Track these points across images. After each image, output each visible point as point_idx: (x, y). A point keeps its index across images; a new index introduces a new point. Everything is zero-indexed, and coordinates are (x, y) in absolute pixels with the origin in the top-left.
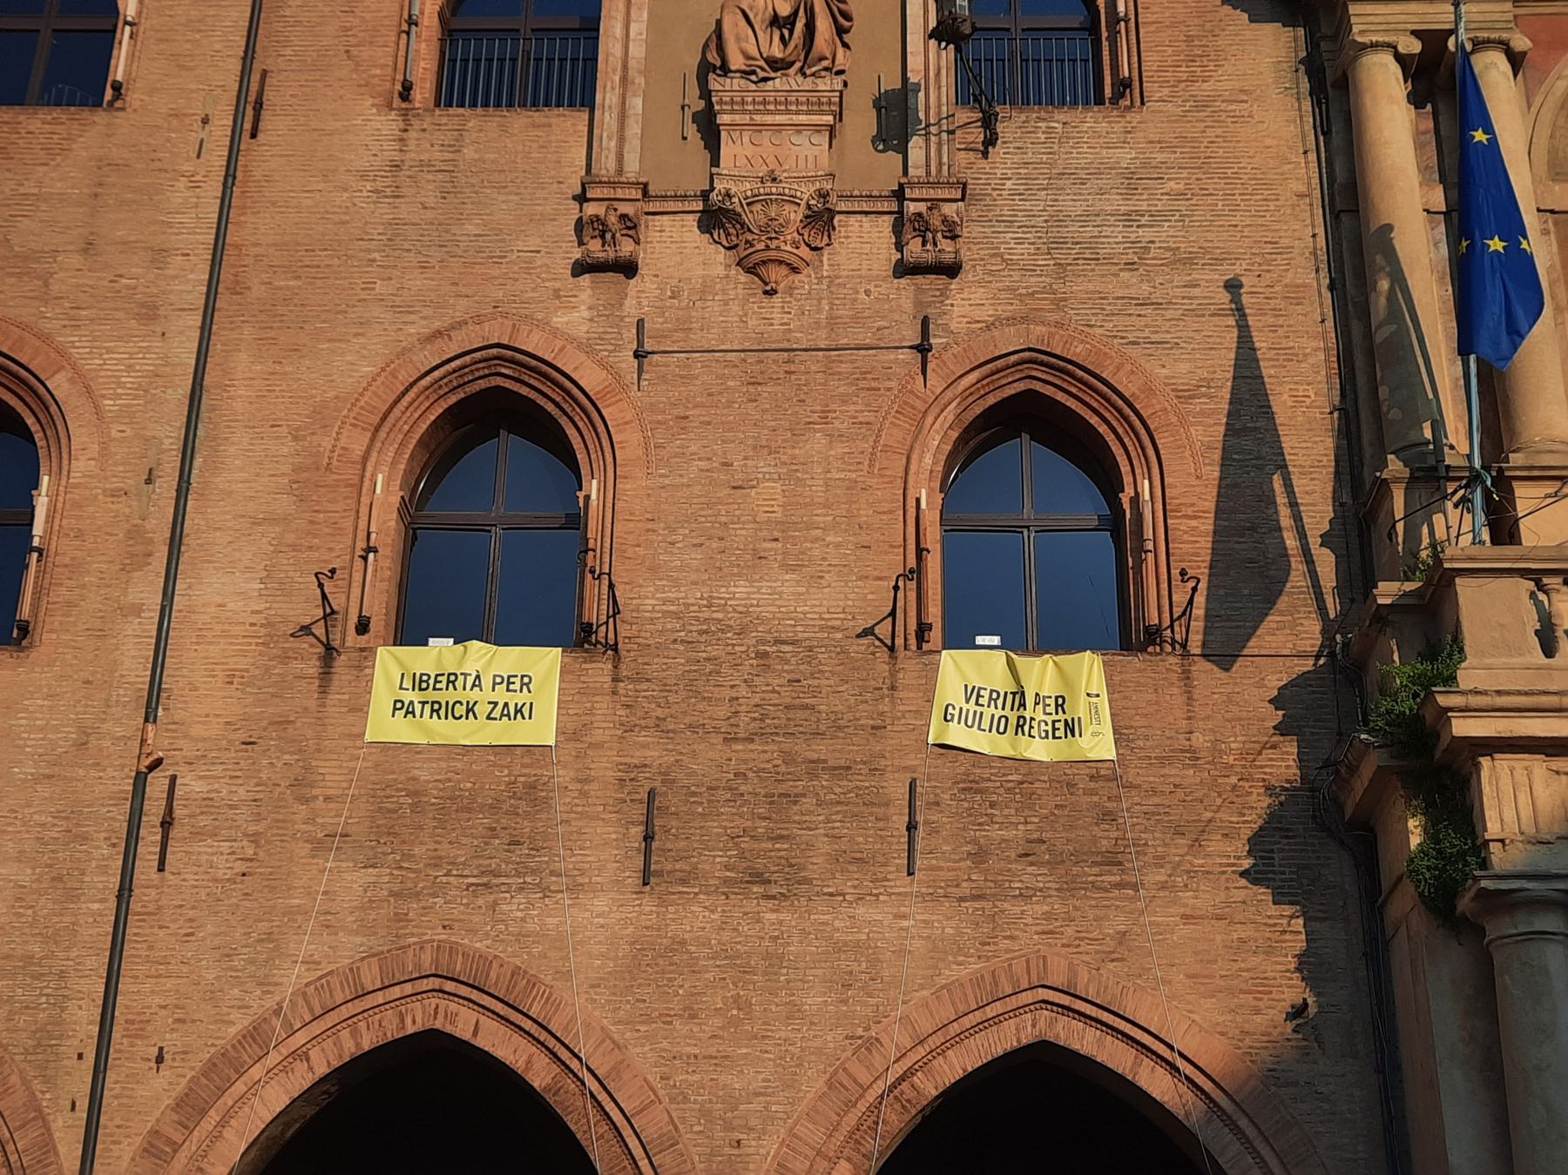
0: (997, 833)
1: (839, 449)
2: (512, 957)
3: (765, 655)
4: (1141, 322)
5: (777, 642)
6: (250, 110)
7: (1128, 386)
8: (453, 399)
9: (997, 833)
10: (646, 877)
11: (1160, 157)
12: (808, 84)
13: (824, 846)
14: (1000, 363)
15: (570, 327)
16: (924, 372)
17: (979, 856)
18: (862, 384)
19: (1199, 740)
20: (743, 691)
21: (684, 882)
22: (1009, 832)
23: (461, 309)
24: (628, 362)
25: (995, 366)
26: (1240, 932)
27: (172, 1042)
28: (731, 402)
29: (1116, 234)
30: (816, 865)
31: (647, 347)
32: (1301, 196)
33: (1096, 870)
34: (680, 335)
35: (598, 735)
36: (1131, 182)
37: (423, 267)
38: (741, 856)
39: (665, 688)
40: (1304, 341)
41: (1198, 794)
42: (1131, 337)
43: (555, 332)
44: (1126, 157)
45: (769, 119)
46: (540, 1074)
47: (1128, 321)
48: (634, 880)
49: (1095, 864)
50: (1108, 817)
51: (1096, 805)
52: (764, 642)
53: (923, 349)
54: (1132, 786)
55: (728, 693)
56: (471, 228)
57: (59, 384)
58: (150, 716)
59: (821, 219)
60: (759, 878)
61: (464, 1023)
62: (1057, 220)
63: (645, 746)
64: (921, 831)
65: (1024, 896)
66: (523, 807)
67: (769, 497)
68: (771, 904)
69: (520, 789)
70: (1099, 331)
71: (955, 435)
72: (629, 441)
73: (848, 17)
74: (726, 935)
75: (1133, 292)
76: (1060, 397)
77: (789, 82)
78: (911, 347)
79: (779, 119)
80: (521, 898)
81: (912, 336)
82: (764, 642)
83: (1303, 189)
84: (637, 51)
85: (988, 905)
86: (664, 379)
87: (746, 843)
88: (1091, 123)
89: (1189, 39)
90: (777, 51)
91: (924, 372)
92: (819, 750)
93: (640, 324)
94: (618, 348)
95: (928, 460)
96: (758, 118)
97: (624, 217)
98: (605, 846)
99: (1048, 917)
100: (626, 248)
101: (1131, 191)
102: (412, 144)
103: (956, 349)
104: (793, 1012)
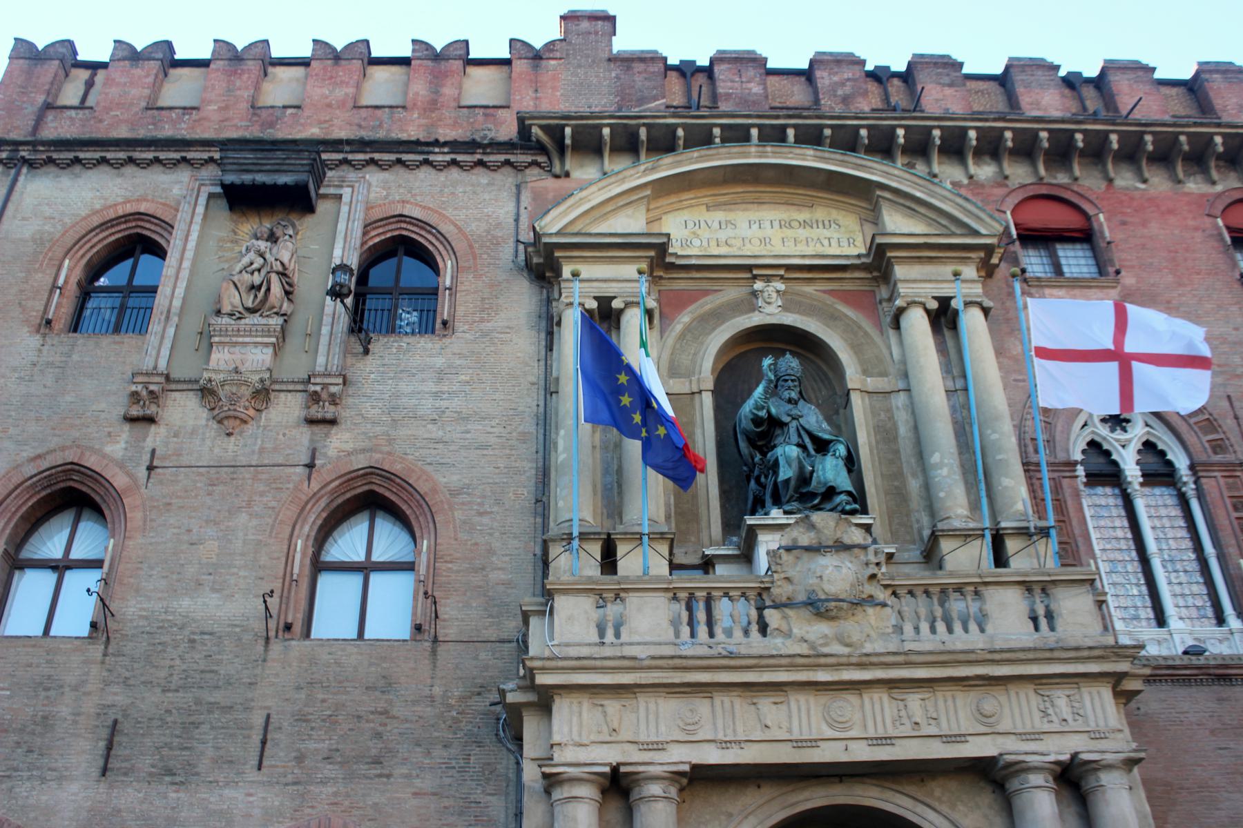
0: (312, 745)
1: (254, 522)
3: (192, 641)
4: (433, 452)
5: (203, 633)
7: (423, 487)
8: (43, 493)
9: (312, 745)
10: (104, 771)
11: (458, 362)
12: (264, 321)
13: (210, 752)
14: (353, 475)
15: (112, 452)
16: (309, 479)
17: (300, 759)
18: (274, 486)
19: (437, 690)
20: (178, 662)
21: (125, 774)
22: (318, 745)
23: (54, 442)
24: (142, 472)
25: (352, 477)
26: (446, 802)
28: (196, 496)
30: (204, 765)
31: (155, 464)
32: (533, 384)
33: (366, 767)
34: (174, 458)
35: (89, 687)
36: (441, 375)
37: (38, 420)
38: (162, 759)
39: (133, 660)
40: (525, 463)
41: (432, 722)
42: (429, 460)
43: (104, 456)
44: (440, 362)
45: (240, 340)
47: (428, 451)
48: (95, 772)
49: (367, 763)
50: (378, 735)
51: (373, 729)
52: (193, 633)
53: (311, 466)
54: (394, 717)
55: (168, 663)
56: (68, 398)
59: (263, 394)
60: (170, 772)
62: (397, 395)
63: (116, 694)
64: (268, 745)
65: (323, 782)
66: (39, 729)
68: (174, 787)
69: (38, 719)
70: (410, 457)
71: (324, 515)
72: (135, 517)
73: (290, 285)
74: (145, 806)
75: (433, 436)
76: (387, 494)
77: (255, 319)
78: (306, 465)
79: (247, 340)
80: (28, 784)
81: (305, 459)
82: (193, 633)
83: (534, 379)
84: (177, 303)
85: (300, 788)
86: (161, 482)
87: (165, 752)
88: (425, 343)
89: (483, 299)
90: (249, 304)
91: (309, 479)
92: (217, 697)
93: (153, 451)
94: (138, 465)
95: (307, 528)
96: (234, 339)
97: (152, 392)
98: (82, 753)
99: (335, 794)
100: (152, 410)
101: (440, 380)
102: (45, 352)
103: (329, 466)
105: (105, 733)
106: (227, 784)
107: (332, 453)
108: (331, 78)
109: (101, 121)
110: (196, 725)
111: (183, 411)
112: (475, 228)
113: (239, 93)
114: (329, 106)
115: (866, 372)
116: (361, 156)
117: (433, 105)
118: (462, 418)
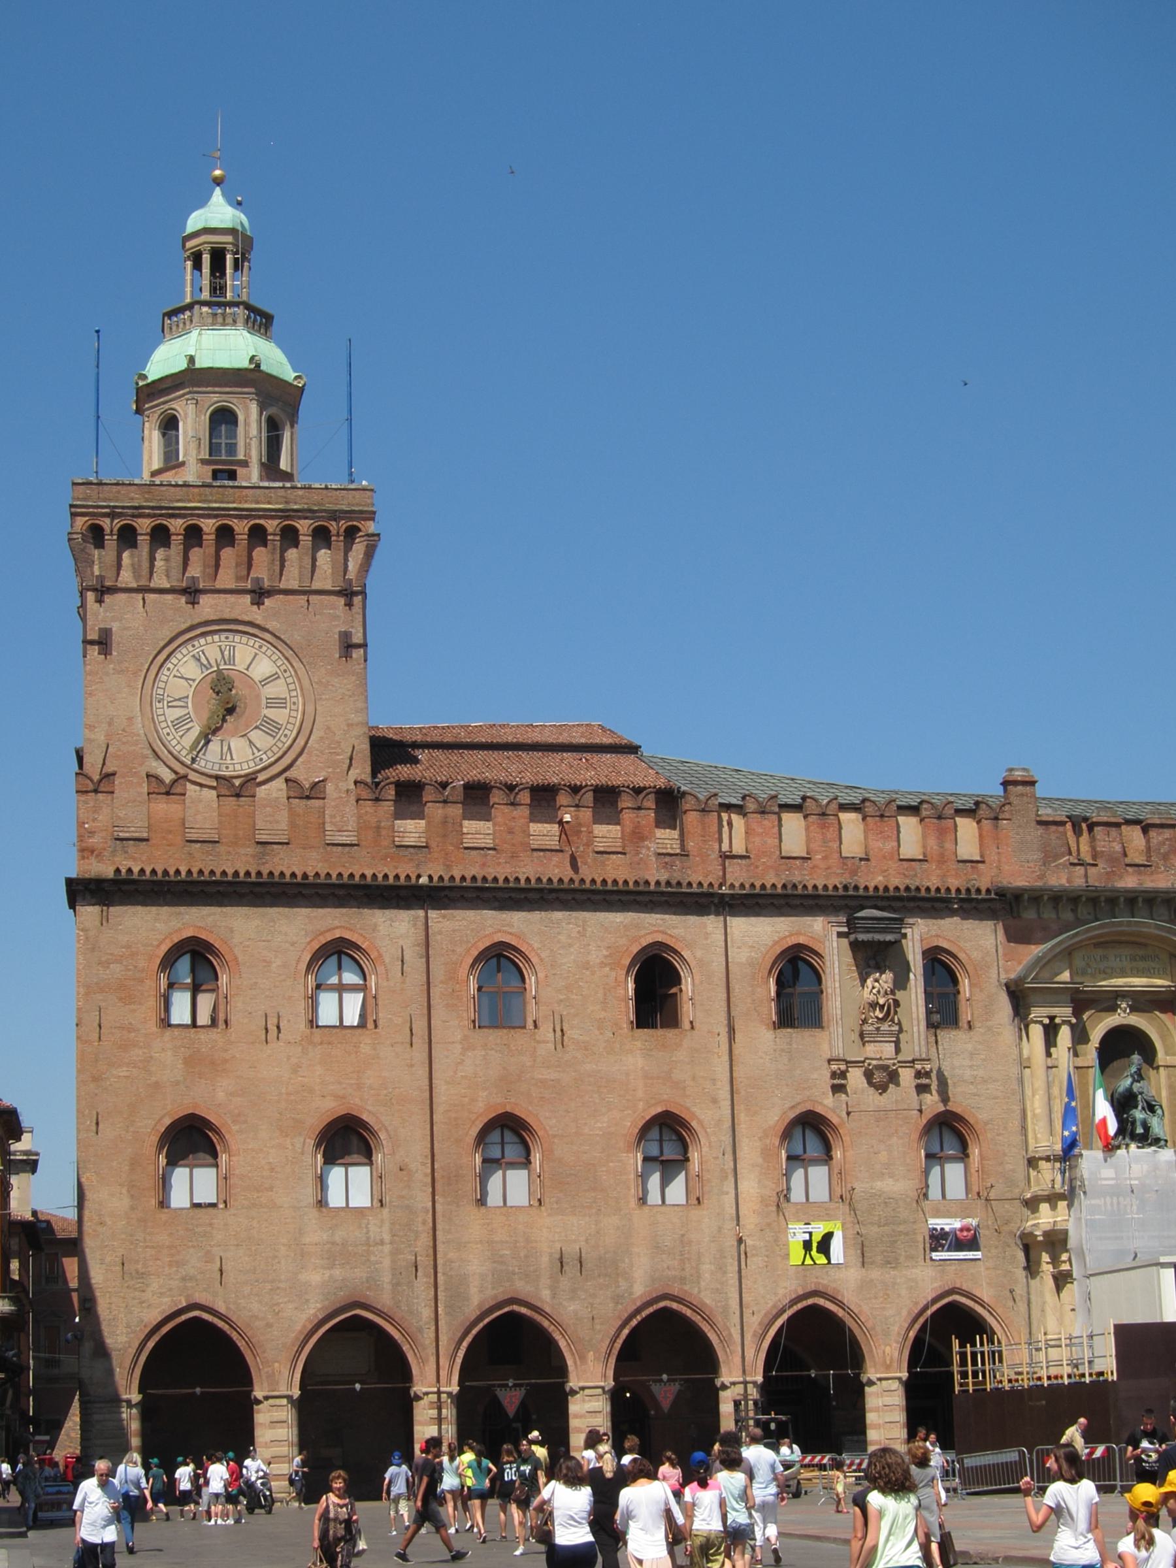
2: (833, 1285)
6: (731, 1031)
7: (972, 1122)
15: (828, 1105)
23: (798, 1099)
24: (844, 1114)
27: (755, 1309)
29: (968, 1072)
30: (902, 1259)
36: (972, 1055)
44: (969, 1047)
46: (841, 1313)
48: (859, 1264)
53: (920, 1111)
57: (694, 1124)
58: (738, 1225)
61: (821, 1302)
67: (883, 1156)
72: (846, 1139)
92: (901, 1228)
104: (899, 1295)
105: (859, 1246)
106: (913, 1267)
107: (929, 1102)
108: (881, 832)
109: (757, 867)
110: (896, 1242)
111: (856, 1078)
112: (975, 955)
113: (830, 844)
114: (885, 857)
115: (1167, 1054)
116: (912, 904)
117: (942, 860)
118: (984, 1081)
